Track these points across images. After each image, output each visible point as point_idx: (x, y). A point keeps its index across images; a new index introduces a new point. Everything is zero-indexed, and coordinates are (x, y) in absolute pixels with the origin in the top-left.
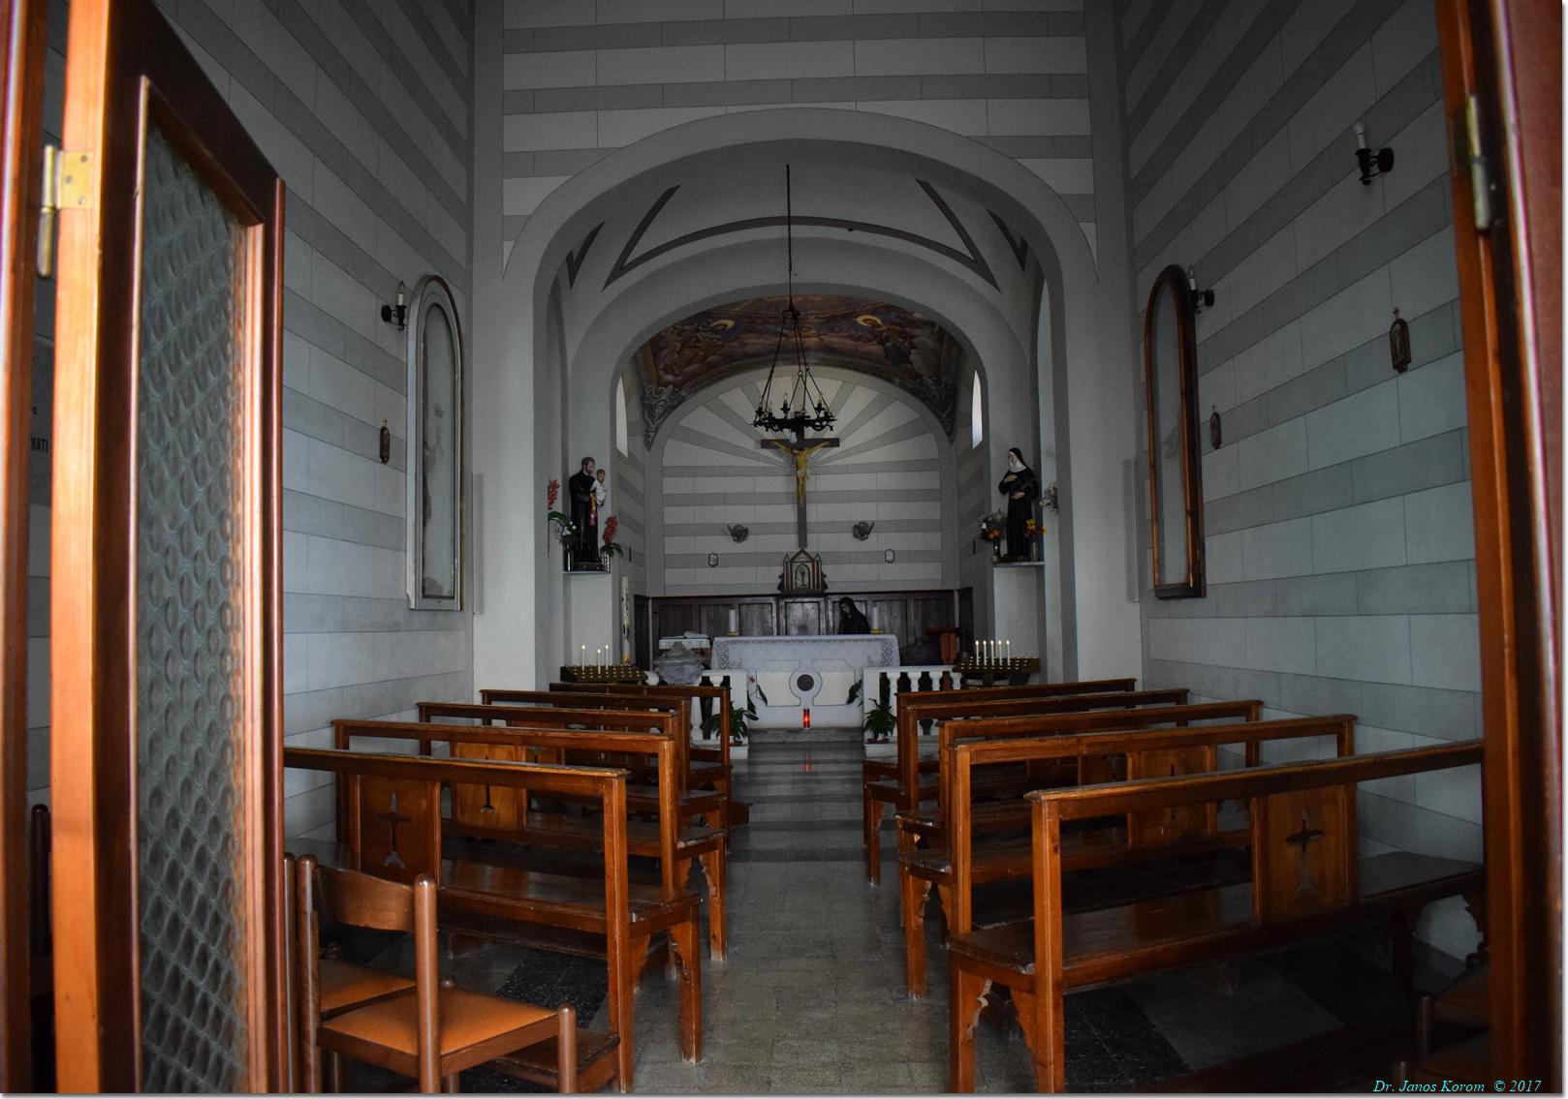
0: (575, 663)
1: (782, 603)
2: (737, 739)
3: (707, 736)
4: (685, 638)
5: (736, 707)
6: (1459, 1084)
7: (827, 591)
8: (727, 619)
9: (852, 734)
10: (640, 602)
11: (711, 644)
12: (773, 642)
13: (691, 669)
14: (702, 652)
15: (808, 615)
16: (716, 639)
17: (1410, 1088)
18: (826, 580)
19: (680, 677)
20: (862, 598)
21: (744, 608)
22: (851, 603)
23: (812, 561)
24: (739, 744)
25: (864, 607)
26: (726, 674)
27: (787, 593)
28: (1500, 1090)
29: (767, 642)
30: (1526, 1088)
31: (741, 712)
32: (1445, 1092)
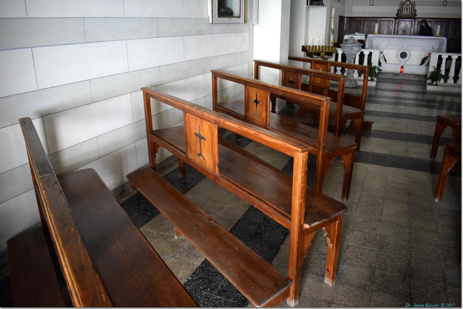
0: (310, 44)
1: (397, 21)
2: (372, 78)
3: (360, 76)
4: (355, 35)
5: (373, 65)
7: (416, 17)
8: (374, 27)
9: (420, 78)
10: (341, 19)
11: (366, 38)
12: (393, 37)
13: (356, 49)
14: (360, 41)
15: (407, 26)
16: (369, 35)
18: (416, 12)
19: (350, 52)
20: (431, 20)
21: (382, 22)
22: (426, 22)
23: (412, 4)
24: (372, 80)
25: (430, 24)
26: (371, 51)
27: (399, 17)
29: (390, 37)
31: (375, 67)
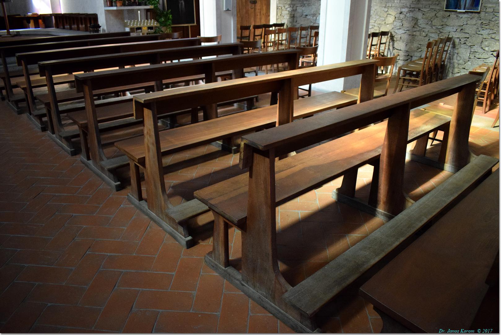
6: (466, 330)
17: (451, 332)
28: (479, 332)
30: (488, 332)
32: (462, 333)
